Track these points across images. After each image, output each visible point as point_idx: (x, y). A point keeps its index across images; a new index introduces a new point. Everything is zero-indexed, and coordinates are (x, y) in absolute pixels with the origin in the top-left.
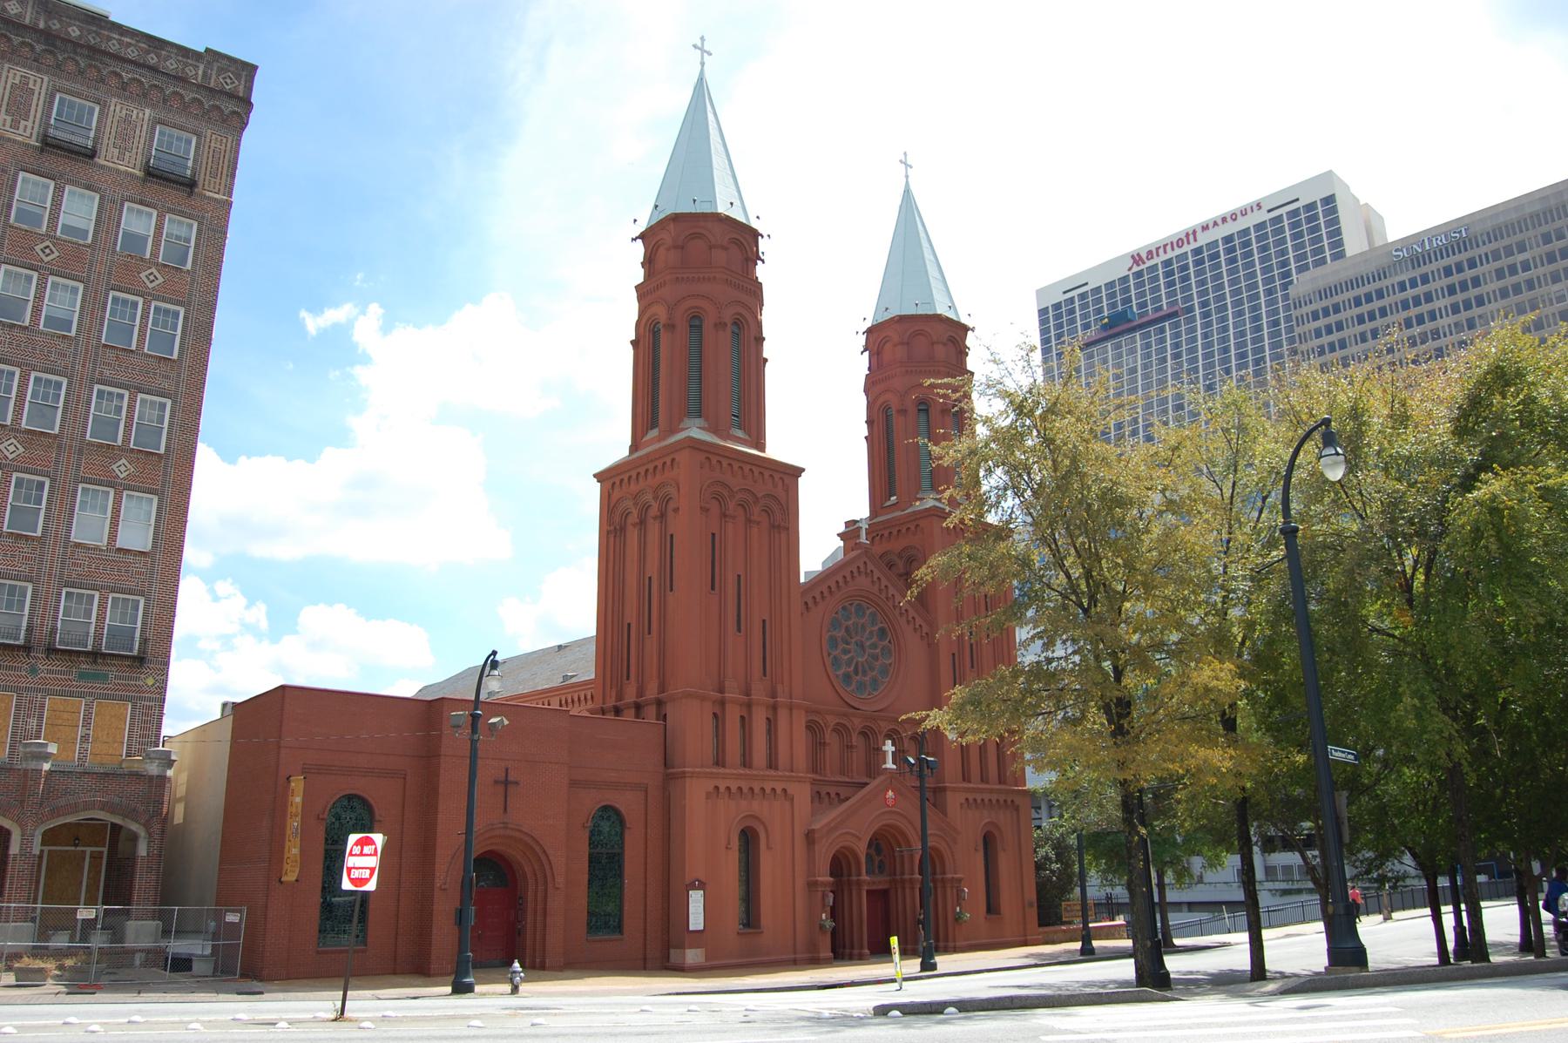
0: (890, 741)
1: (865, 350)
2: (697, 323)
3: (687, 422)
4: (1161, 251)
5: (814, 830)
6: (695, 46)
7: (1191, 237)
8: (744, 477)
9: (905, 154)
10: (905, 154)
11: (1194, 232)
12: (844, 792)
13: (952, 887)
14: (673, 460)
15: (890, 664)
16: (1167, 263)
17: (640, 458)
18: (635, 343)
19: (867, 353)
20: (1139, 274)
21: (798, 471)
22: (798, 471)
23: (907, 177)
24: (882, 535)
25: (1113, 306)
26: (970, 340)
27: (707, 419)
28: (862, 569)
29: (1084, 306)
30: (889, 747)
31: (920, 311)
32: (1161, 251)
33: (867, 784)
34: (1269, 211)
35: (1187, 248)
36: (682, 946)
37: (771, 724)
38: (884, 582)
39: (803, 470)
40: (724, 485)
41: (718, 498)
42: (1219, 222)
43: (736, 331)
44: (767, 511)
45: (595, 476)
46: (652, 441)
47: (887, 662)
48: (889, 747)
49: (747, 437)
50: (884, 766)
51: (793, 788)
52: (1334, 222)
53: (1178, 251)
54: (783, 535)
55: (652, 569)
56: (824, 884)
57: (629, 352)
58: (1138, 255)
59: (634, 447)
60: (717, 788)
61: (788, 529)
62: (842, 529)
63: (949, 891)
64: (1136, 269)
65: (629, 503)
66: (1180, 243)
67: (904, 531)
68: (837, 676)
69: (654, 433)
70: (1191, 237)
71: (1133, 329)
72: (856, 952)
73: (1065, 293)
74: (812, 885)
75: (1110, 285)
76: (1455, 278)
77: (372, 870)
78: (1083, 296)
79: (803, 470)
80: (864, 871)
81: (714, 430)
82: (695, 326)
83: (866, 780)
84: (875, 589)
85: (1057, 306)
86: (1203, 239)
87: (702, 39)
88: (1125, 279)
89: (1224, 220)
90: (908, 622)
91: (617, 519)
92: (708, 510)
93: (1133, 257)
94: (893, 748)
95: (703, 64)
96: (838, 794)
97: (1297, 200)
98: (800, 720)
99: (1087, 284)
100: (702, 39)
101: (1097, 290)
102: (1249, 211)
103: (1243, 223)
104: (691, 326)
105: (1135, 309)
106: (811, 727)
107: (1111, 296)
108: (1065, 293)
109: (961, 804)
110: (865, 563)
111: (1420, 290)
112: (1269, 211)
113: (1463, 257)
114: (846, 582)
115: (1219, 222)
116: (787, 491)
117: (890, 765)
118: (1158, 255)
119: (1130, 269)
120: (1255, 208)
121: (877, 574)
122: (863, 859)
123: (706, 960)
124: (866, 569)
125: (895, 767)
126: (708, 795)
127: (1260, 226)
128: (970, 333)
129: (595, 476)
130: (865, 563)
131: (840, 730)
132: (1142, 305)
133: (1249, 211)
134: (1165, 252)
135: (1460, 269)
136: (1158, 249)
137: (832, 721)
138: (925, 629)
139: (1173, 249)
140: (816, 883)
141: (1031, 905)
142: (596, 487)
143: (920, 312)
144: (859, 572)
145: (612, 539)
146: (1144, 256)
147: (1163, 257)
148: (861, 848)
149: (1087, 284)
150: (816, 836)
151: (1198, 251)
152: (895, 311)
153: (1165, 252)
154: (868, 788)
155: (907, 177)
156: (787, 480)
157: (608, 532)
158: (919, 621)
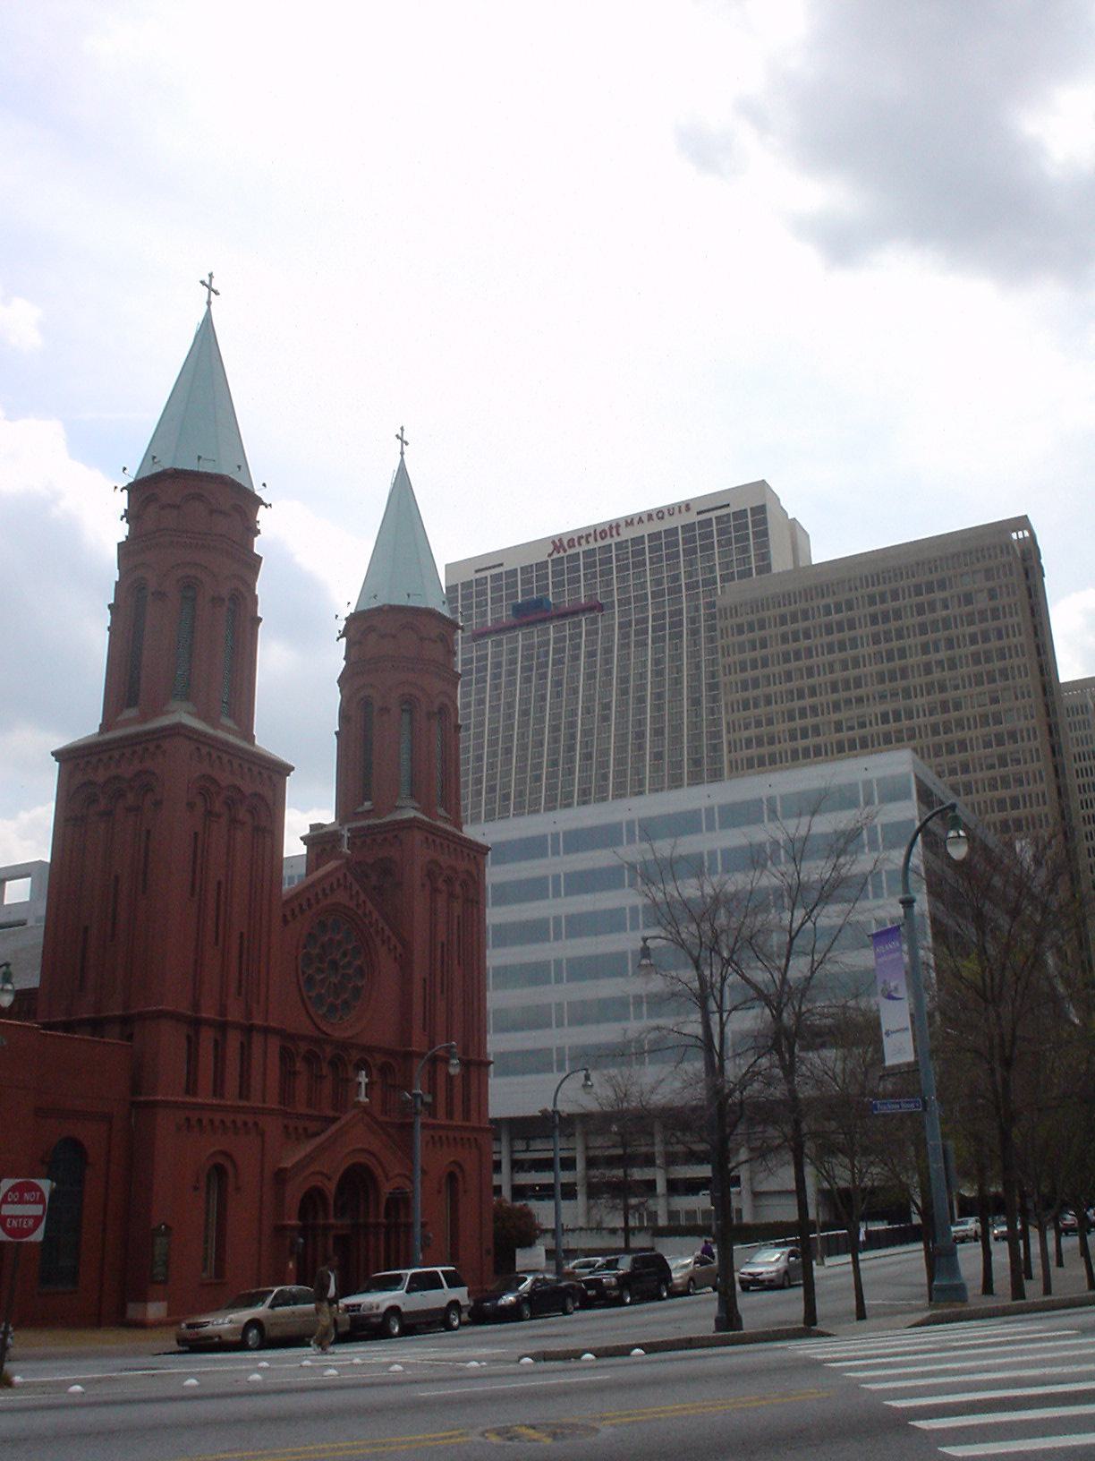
0: (364, 1072)
1: (341, 637)
3: (174, 705)
4: (583, 541)
5: (286, 1169)
6: (203, 283)
7: (614, 532)
9: (402, 429)
10: (402, 429)
11: (618, 526)
16: (588, 553)
17: (115, 741)
19: (344, 640)
21: (284, 770)
23: (402, 453)
28: (342, 881)
29: (496, 589)
30: (363, 1078)
31: (412, 603)
32: (583, 541)
33: (339, 1118)
34: (699, 513)
35: (608, 541)
36: (143, 1298)
37: (245, 1049)
38: (362, 897)
39: (293, 769)
40: (215, 782)
42: (645, 518)
45: (53, 754)
46: (127, 722)
48: (363, 1078)
50: (356, 1099)
52: (762, 534)
53: (601, 543)
56: (293, 1228)
58: (560, 540)
59: (105, 727)
60: (188, 1120)
62: (307, 831)
64: (555, 556)
66: (603, 534)
68: (310, 998)
69: (131, 713)
70: (614, 532)
73: (477, 571)
74: (280, 1230)
77: (37, 1219)
78: (496, 578)
79: (293, 769)
80: (332, 1213)
81: (205, 718)
83: (330, 1113)
85: (466, 585)
86: (627, 534)
87: (211, 275)
89: (650, 516)
90: (383, 942)
93: (554, 542)
95: (209, 303)
96: (305, 1129)
98: (274, 1045)
99: (501, 565)
100: (211, 275)
101: (513, 573)
103: (669, 523)
105: (551, 600)
106: (286, 1056)
108: (477, 571)
110: (345, 874)
112: (699, 513)
114: (326, 895)
115: (645, 518)
117: (363, 1099)
118: (580, 544)
119: (550, 555)
123: (168, 1315)
125: (367, 1100)
127: (688, 528)
129: (53, 754)
130: (345, 874)
131: (311, 1059)
134: (588, 542)
136: (580, 538)
137: (303, 1047)
139: (596, 540)
140: (284, 1227)
144: (339, 885)
146: (566, 547)
147: (585, 547)
148: (331, 1187)
149: (501, 565)
151: (619, 545)
152: (382, 600)
153: (588, 542)
155: (402, 453)
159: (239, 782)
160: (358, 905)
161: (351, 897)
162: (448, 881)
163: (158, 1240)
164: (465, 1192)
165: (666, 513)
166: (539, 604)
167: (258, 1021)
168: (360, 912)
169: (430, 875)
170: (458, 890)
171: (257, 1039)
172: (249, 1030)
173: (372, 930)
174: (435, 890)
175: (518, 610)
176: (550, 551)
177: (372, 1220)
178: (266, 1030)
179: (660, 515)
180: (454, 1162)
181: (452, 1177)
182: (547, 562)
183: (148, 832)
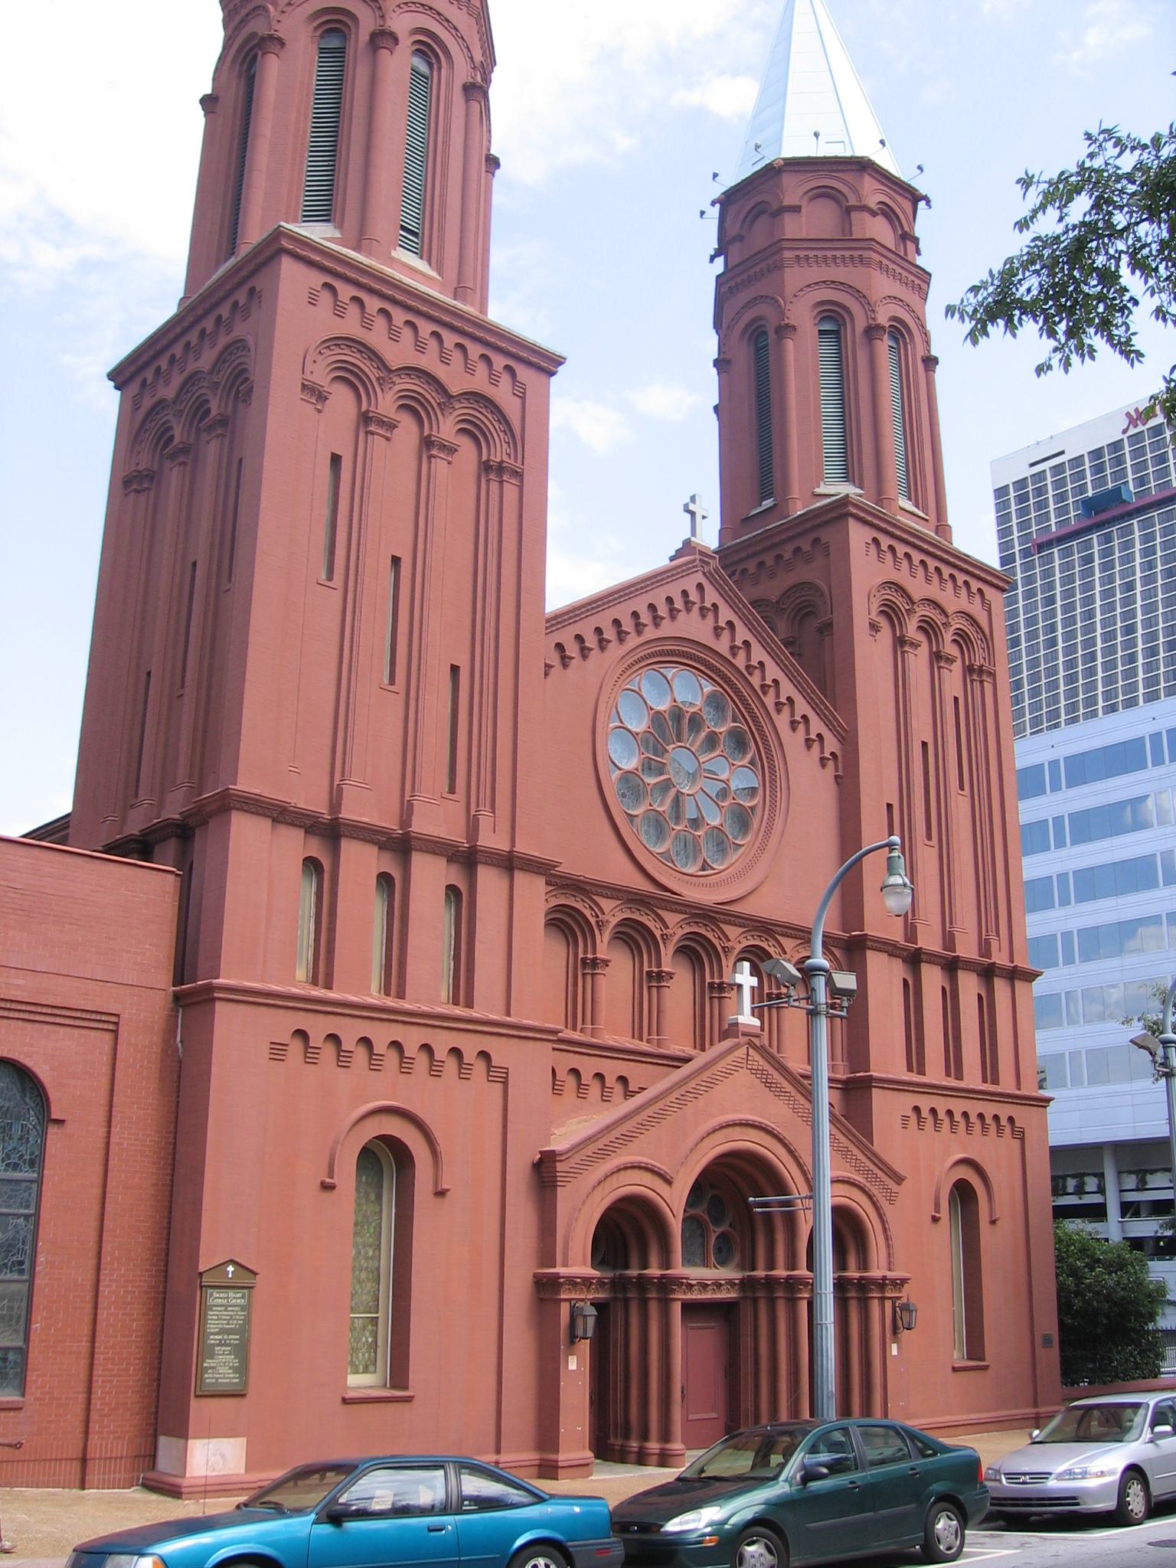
0: (746, 965)
2: (334, 42)
8: (420, 347)
12: (635, 1072)
13: (882, 1299)
14: (252, 291)
15: (753, 808)
18: (208, 102)
19: (720, 261)
20: (1136, 438)
21: (547, 364)
22: (547, 364)
24: (744, 571)
25: (1100, 482)
26: (925, 224)
27: (340, 226)
28: (694, 596)
29: (1059, 484)
33: (687, 1060)
38: (742, 634)
40: (374, 355)
41: (350, 377)
43: (423, 68)
44: (473, 431)
47: (747, 804)
49: (434, 274)
51: (503, 1052)
54: (510, 491)
55: (201, 551)
57: (196, 121)
61: (518, 475)
63: (875, 1306)
64: (1132, 431)
67: (787, 555)
71: (1130, 515)
72: (654, 1446)
73: (1032, 465)
74: (546, 1288)
75: (1097, 454)
78: (1058, 469)
79: (558, 361)
83: (689, 1051)
84: (723, 646)
85: (1021, 484)
88: (1116, 446)
90: (794, 725)
92: (321, 397)
93: (1128, 415)
94: (754, 981)
96: (623, 1080)
99: (1062, 453)
101: (1078, 461)
107: (1098, 469)
108: (1032, 465)
109: (905, 1118)
116: (523, 398)
117: (747, 1019)
119: (1125, 431)
121: (726, 614)
122: (676, 1226)
123: (249, 1468)
124: (703, 600)
125: (756, 1022)
126: (278, 1051)
128: (922, 204)
132: (1141, 481)
137: (613, 912)
138: (831, 744)
141: (1047, 1340)
142: (110, 400)
143: (821, 154)
144: (688, 604)
148: (673, 1202)
149: (1062, 453)
150: (559, 1167)
154: (687, 1069)
156: (523, 373)
157: (127, 482)
158: (817, 726)
159: (428, 361)
160: (733, 649)
161: (717, 631)
162: (928, 628)
163: (216, 1298)
164: (993, 1222)
166: (1115, 496)
167: (492, 839)
168: (740, 661)
169: (889, 612)
170: (951, 649)
171: (489, 880)
172: (468, 858)
173: (769, 700)
174: (901, 642)
175: (1090, 506)
176: (1125, 427)
177: (781, 1272)
178: (510, 863)
180: (966, 1162)
181: (963, 1193)
182: (1122, 440)
183: (241, 461)
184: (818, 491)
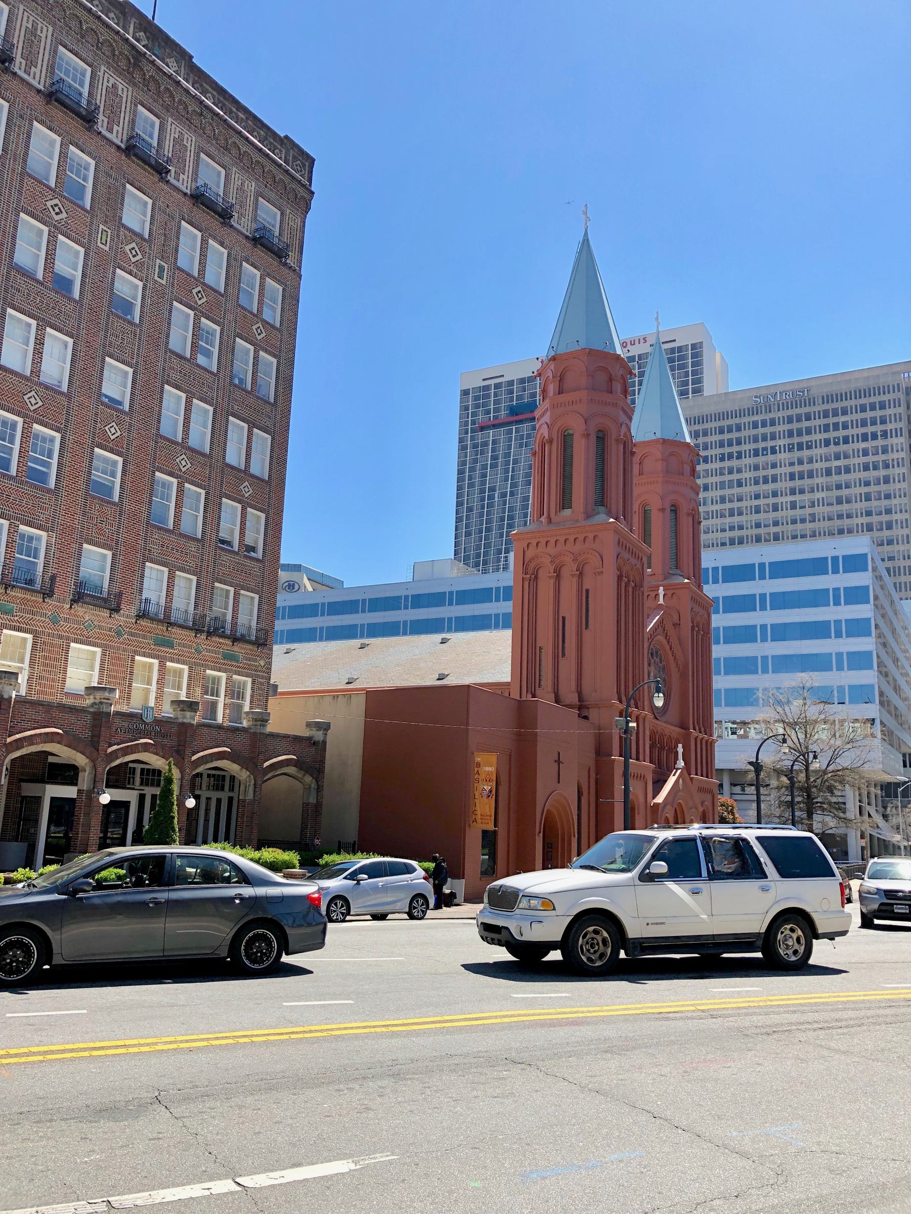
52: (697, 364)
65: (547, 560)
73: (484, 380)
75: (522, 381)
76: (795, 426)
78: (497, 386)
82: (600, 438)
91: (530, 571)
97: (674, 341)
99: (503, 376)
101: (511, 383)
102: (637, 342)
104: (597, 437)
108: (484, 380)
111: (768, 430)
113: (802, 411)
120: (642, 341)
133: (637, 342)
135: (799, 420)
145: (526, 584)
149: (503, 376)
165: (629, 343)
175: (513, 411)
179: (625, 344)
184: (671, 572)
